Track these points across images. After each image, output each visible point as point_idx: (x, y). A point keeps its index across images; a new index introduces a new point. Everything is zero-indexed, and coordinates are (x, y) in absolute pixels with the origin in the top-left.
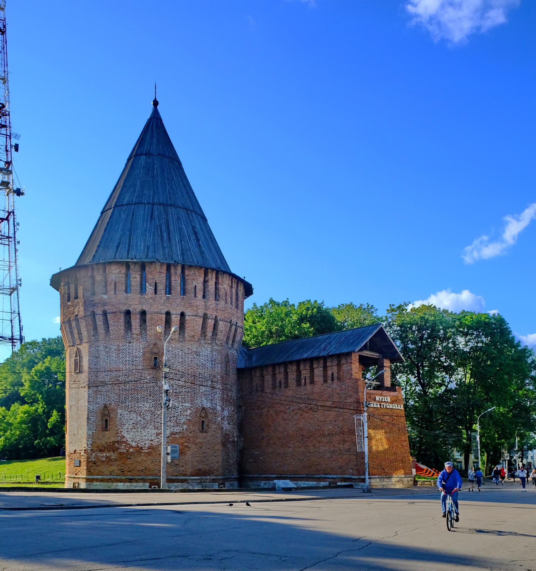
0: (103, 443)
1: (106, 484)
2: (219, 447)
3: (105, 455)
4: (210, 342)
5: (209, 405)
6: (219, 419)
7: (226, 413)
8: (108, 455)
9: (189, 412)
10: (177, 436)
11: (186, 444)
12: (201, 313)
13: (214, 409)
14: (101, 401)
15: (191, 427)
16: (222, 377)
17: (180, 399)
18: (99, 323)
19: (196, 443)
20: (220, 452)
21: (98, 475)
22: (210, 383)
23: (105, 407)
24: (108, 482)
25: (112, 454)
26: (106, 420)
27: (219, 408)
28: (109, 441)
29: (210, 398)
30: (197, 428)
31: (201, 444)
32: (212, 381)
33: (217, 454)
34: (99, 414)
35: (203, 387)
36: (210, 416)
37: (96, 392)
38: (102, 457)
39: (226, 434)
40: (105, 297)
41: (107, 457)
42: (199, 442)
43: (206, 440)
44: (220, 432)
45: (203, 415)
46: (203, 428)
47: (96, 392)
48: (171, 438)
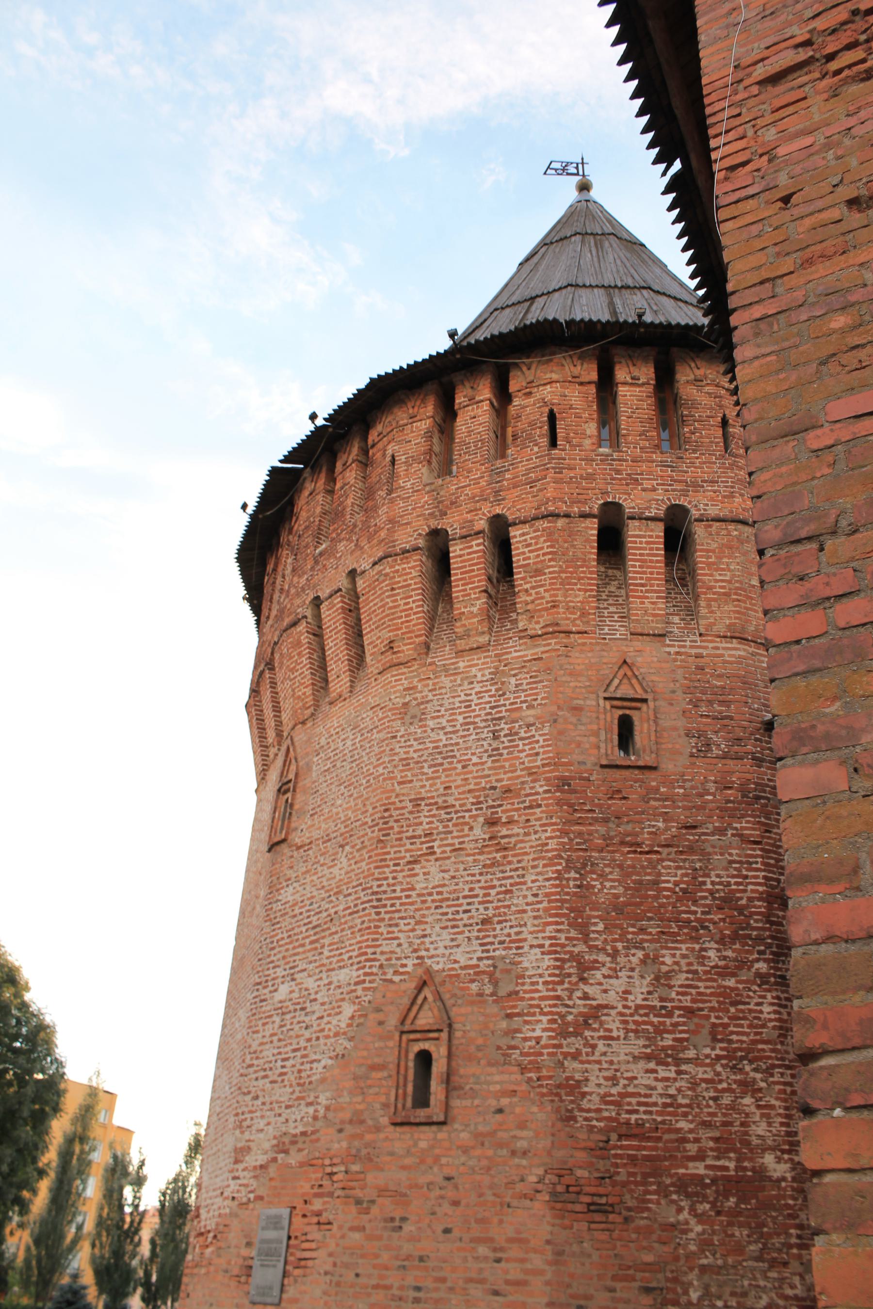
2: (536, 1220)
4: (483, 639)
5: (467, 954)
6: (539, 1029)
7: (620, 986)
9: (348, 1010)
10: (294, 1159)
11: (317, 1205)
12: (412, 534)
13: (498, 975)
15: (346, 1099)
16: (563, 783)
17: (326, 953)
19: (368, 1193)
20: (537, 1261)
22: (479, 832)
27: (536, 963)
29: (479, 912)
30: (384, 1092)
31: (400, 1196)
32: (492, 822)
33: (514, 1272)
35: (433, 868)
36: (469, 1021)
39: (628, 1132)
42: (382, 1191)
43: (436, 1175)
44: (540, 1114)
45: (426, 1018)
46: (422, 1099)
48: (272, 1171)
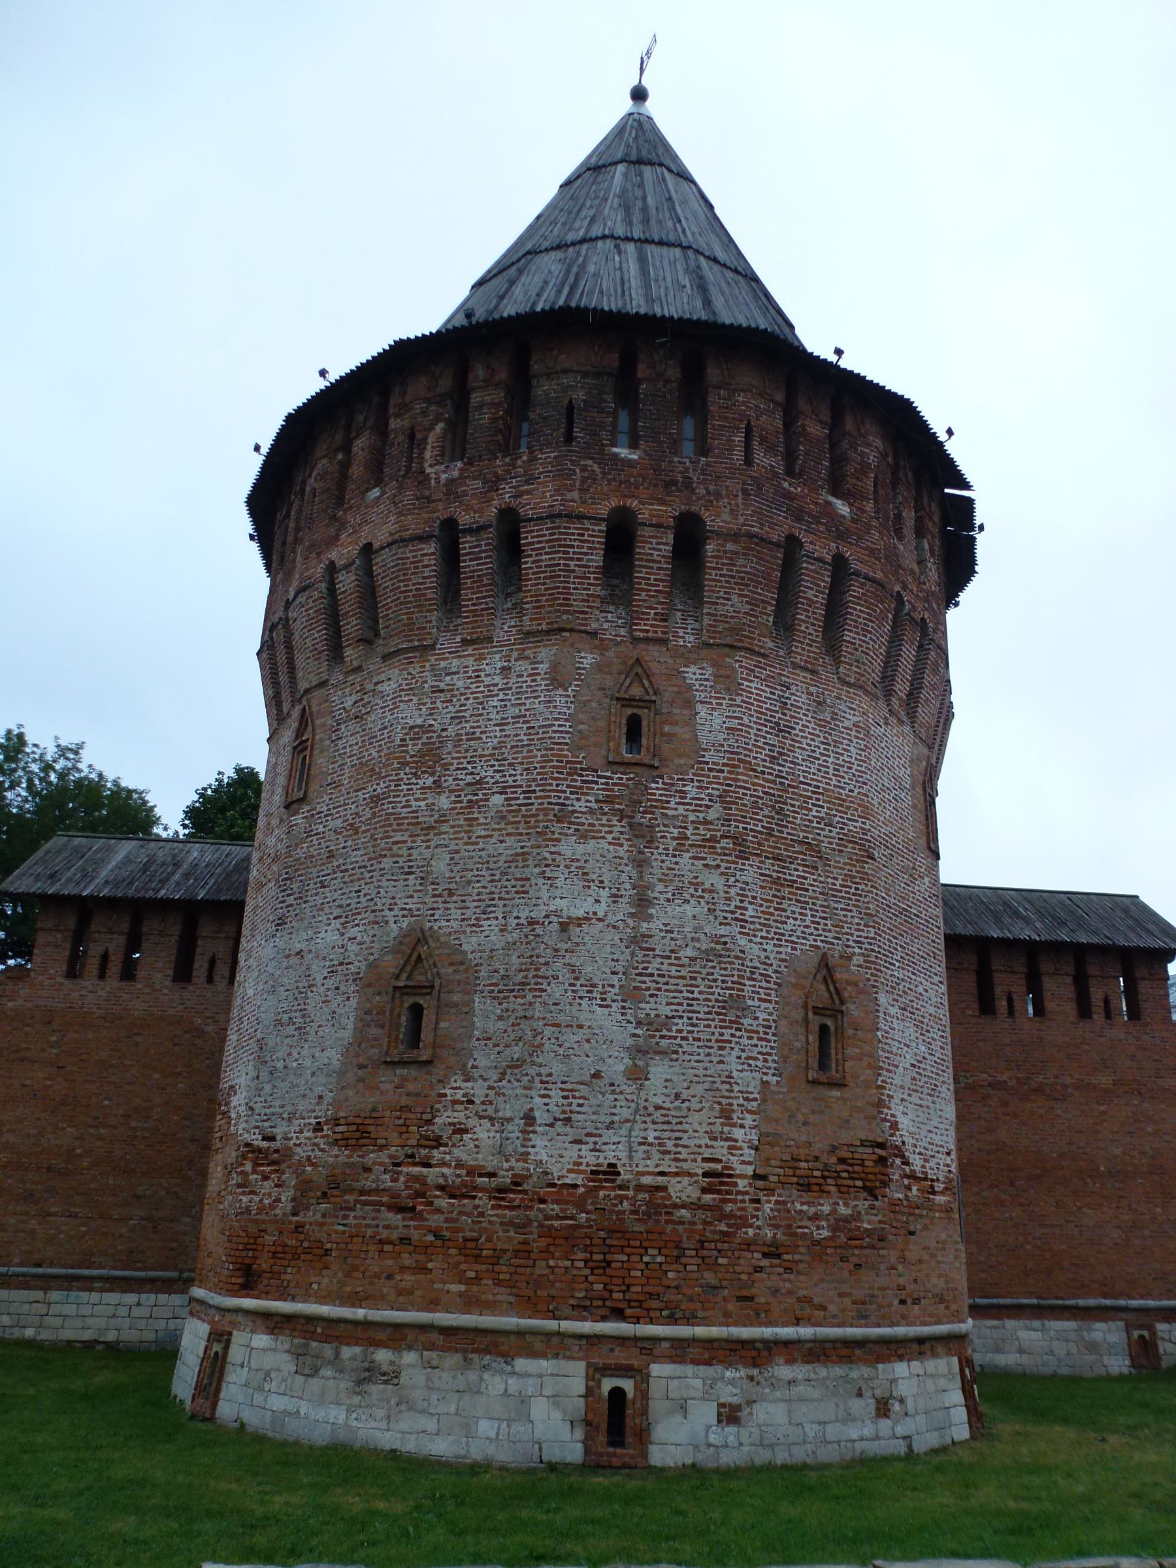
0: (819, 1147)
1: (838, 1370)
3: (826, 1209)
8: (843, 1210)
14: (802, 933)
18: (810, 594)
21: (798, 1321)
23: (826, 968)
24: (848, 1359)
25: (863, 1205)
26: (824, 1029)
28: (845, 1137)
34: (797, 997)
37: (777, 882)
38: (815, 1217)
40: (842, 508)
41: (839, 1224)
47: (777, 882)
